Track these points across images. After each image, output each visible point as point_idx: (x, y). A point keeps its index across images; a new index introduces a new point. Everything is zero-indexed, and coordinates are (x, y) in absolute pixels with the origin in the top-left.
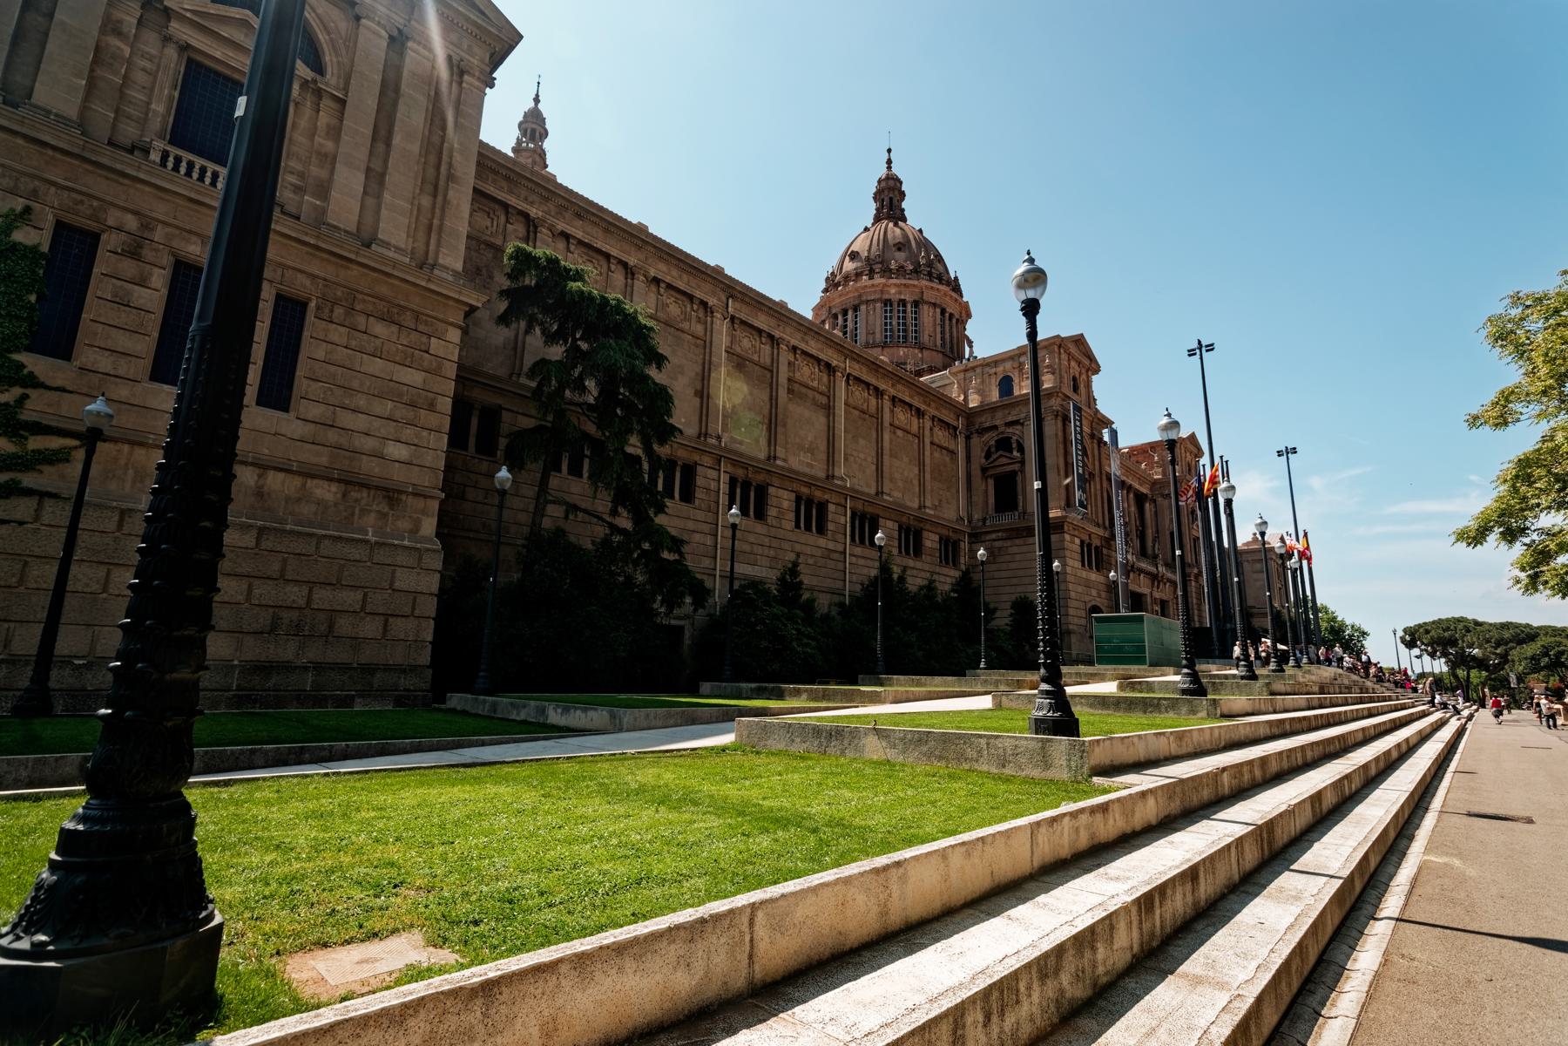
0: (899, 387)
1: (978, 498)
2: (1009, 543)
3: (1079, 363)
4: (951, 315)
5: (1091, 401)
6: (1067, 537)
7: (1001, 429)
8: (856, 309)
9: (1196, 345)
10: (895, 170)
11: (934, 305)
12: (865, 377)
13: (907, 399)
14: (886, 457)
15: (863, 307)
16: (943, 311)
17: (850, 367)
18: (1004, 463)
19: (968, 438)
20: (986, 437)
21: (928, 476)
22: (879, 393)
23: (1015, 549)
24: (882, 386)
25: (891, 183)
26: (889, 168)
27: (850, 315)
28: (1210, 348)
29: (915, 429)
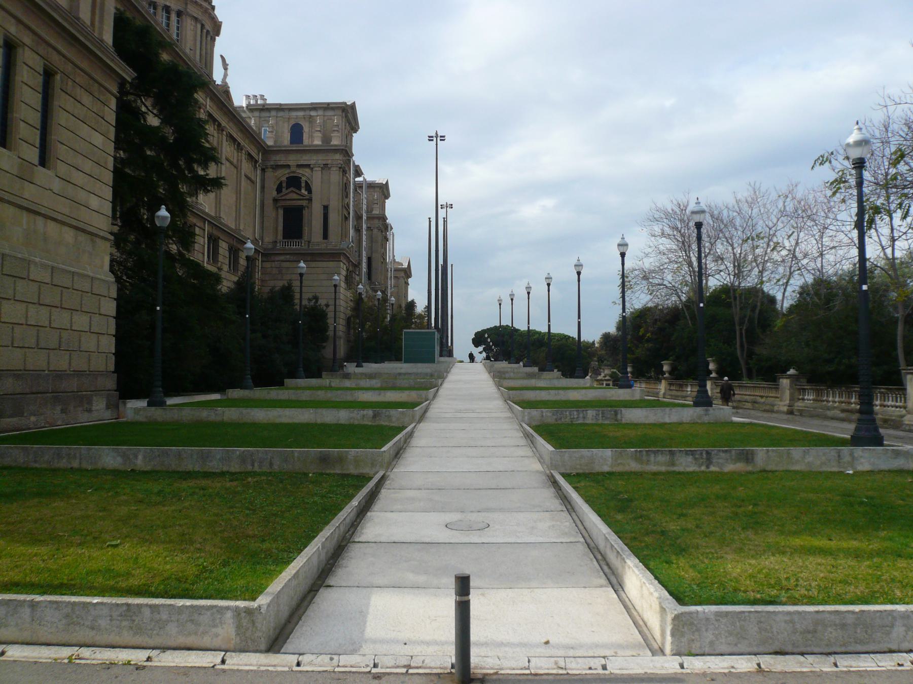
0: (231, 124)
4: (208, 31)
7: (293, 169)
9: (434, 135)
11: (196, 19)
13: (235, 136)
18: (292, 197)
19: (263, 170)
24: (224, 124)
28: (443, 138)
29: (235, 162)
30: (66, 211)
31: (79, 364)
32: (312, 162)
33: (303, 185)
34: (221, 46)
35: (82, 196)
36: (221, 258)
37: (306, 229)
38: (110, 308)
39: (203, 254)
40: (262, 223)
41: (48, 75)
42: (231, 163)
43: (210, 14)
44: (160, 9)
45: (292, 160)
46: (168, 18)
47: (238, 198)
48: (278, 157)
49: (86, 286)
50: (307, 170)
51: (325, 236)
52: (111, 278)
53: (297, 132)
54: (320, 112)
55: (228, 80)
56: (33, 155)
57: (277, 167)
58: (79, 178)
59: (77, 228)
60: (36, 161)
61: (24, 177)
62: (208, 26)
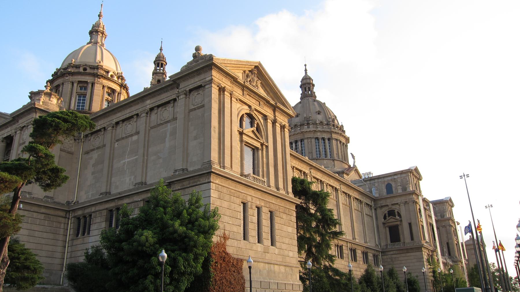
3: (416, 177)
4: (343, 143)
7: (390, 206)
8: (302, 141)
10: (309, 74)
11: (337, 140)
12: (346, 191)
15: (306, 141)
18: (392, 221)
19: (375, 209)
21: (366, 229)
22: (349, 197)
24: (351, 194)
25: (308, 81)
26: (306, 73)
27: (299, 143)
30: (281, 260)
32: (399, 202)
33: (396, 214)
34: (351, 148)
35: (286, 252)
36: (358, 258)
37: (401, 236)
39: (348, 258)
40: (379, 236)
41: (271, 212)
43: (343, 136)
45: (389, 202)
46: (324, 143)
48: (382, 202)
50: (398, 206)
51: (412, 239)
52: (300, 283)
53: (389, 188)
54: (399, 176)
55: (356, 164)
56: (267, 242)
57: (382, 207)
58: (284, 246)
59: (285, 266)
61: (266, 252)
62: (343, 140)
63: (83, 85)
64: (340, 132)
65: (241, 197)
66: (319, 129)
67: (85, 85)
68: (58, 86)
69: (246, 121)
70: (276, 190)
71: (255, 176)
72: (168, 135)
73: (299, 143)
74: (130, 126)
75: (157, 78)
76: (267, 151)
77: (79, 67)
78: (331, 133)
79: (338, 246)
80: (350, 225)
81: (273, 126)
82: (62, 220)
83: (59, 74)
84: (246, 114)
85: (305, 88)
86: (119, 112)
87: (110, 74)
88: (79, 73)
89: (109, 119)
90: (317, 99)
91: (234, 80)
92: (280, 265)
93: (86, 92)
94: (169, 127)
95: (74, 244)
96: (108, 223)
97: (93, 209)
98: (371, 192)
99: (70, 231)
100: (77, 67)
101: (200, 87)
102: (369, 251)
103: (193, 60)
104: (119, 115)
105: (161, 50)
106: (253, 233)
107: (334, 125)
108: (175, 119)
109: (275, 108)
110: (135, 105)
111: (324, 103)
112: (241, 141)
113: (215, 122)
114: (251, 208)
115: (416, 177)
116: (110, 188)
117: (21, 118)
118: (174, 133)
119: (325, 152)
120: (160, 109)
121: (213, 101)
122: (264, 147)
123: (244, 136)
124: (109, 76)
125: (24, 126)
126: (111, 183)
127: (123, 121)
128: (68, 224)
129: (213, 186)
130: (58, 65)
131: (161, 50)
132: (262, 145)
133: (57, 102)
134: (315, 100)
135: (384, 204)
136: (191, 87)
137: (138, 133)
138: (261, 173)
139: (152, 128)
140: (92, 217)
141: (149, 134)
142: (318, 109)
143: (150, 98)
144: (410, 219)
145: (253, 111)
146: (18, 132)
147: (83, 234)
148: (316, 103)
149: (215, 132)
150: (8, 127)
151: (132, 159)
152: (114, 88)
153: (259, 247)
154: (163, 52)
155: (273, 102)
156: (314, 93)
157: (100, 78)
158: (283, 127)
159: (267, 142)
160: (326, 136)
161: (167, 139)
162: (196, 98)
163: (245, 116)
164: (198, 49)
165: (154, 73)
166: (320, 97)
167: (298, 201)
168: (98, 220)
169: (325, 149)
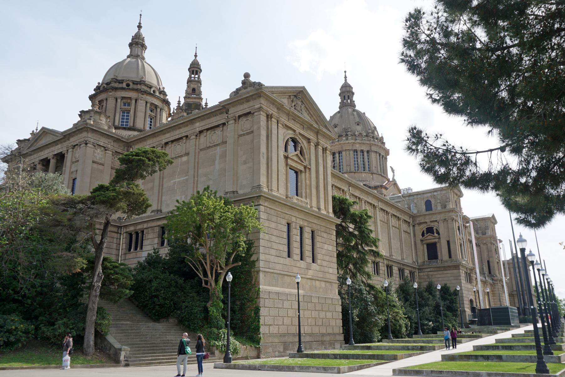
0: (393, 209)
1: (420, 253)
2: (435, 273)
3: (456, 194)
4: (383, 156)
5: (461, 209)
6: (461, 271)
8: (340, 153)
10: (348, 81)
12: (384, 208)
13: (395, 214)
14: (392, 240)
15: (344, 153)
16: (380, 154)
17: (381, 205)
18: (430, 239)
19: (414, 226)
20: (422, 226)
21: (404, 245)
23: (439, 276)
24: (389, 211)
25: (348, 89)
26: (346, 80)
27: (337, 155)
29: (397, 226)
30: (322, 276)
31: (330, 331)
32: (438, 219)
35: (326, 269)
37: (439, 254)
38: (340, 309)
40: (416, 252)
42: (395, 227)
44: (359, 153)
46: (363, 155)
47: (401, 244)
48: (420, 219)
49: (330, 302)
51: (450, 256)
53: (428, 205)
54: (439, 193)
56: (310, 260)
57: (420, 224)
58: (325, 264)
59: (325, 281)
60: (311, 261)
61: (308, 269)
62: (383, 153)
63: (127, 101)
64: (379, 144)
65: (286, 218)
66: (358, 141)
67: (129, 101)
68: (100, 102)
69: (291, 144)
70: (318, 210)
71: (298, 198)
72: (218, 158)
73: (337, 155)
74: (178, 147)
75: (192, 86)
76: (310, 174)
77: (122, 83)
78: (371, 145)
79: (374, 262)
80: (387, 241)
81: (315, 149)
82: (115, 235)
83: (101, 89)
84: (291, 138)
85: (344, 97)
86: (168, 132)
87: (152, 90)
88: (123, 89)
89: (158, 139)
90: (356, 108)
91: (280, 108)
92: (321, 281)
93: (129, 107)
94: (219, 150)
95: (127, 258)
96: (160, 239)
97: (145, 226)
98: (410, 208)
99: (123, 245)
100: (121, 82)
101: (249, 113)
102: (405, 267)
103: (242, 86)
104: (168, 135)
105: (196, 56)
106: (296, 251)
107: (373, 137)
108: (225, 143)
109: (317, 133)
110: (184, 126)
111: (364, 113)
112: (287, 164)
113: (263, 149)
114: (296, 228)
115: (456, 194)
116: (161, 206)
117: (73, 136)
118: (224, 156)
119: (364, 165)
120: (209, 132)
121: (262, 128)
122: (307, 170)
123: (289, 160)
124: (152, 92)
125: (77, 145)
126: (161, 201)
127: (172, 141)
128: (120, 239)
129: (262, 208)
130: (98, 78)
131: (196, 56)
132: (305, 167)
133: (106, 121)
134: (354, 110)
135: (422, 221)
136: (241, 113)
137: (187, 154)
138: (304, 195)
139: (201, 150)
140: (145, 233)
141: (198, 156)
142: (357, 120)
143: (199, 121)
144: (449, 236)
145: (297, 135)
146: (69, 151)
147: (136, 249)
148: (355, 113)
149: (263, 157)
150: (58, 144)
151: (182, 179)
152: (156, 103)
153: (302, 264)
154: (197, 58)
155: (315, 126)
156: (354, 101)
157: (142, 94)
158: (325, 150)
159: (310, 165)
160: (365, 148)
161: (217, 162)
162: (245, 124)
163: (290, 140)
164: (247, 76)
165: (189, 81)
166: (359, 107)
167: (339, 221)
168: (150, 236)
169: (364, 161)
